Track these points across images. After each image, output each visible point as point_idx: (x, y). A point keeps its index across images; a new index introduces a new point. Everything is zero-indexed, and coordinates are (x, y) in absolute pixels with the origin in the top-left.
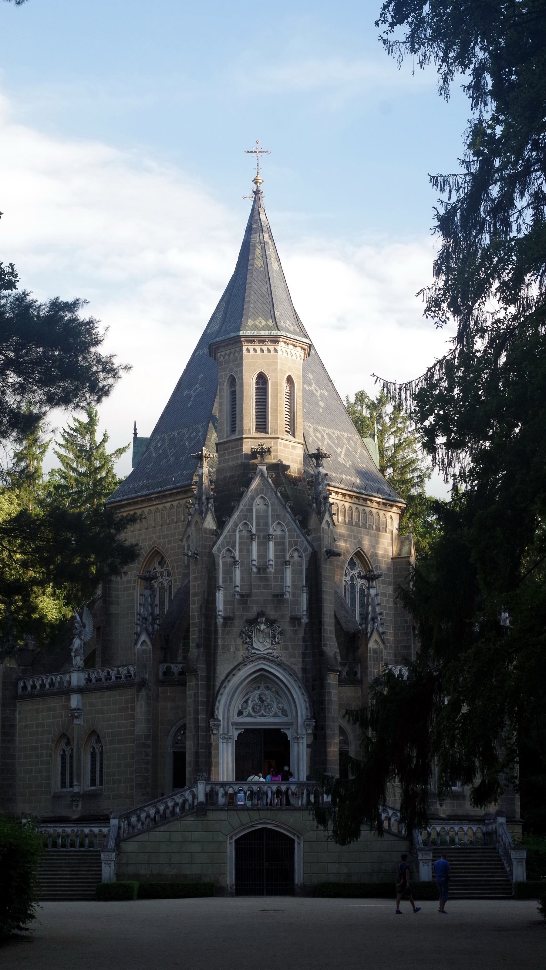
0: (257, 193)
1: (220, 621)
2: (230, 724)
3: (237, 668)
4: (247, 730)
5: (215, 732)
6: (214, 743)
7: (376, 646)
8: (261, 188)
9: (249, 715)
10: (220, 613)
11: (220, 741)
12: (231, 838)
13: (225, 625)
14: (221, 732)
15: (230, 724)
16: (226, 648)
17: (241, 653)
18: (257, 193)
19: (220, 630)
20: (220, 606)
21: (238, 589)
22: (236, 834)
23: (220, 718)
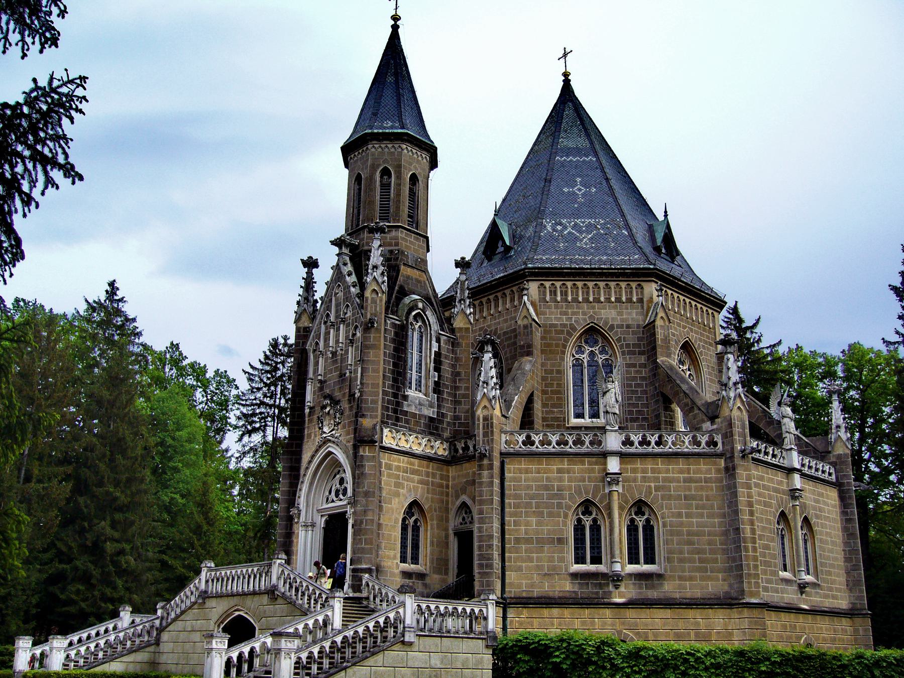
0: (395, 28)
1: (307, 411)
2: (315, 510)
3: (313, 457)
4: (330, 515)
5: (296, 520)
6: (296, 532)
7: (486, 412)
8: (398, 23)
9: (333, 501)
10: (309, 404)
11: (300, 529)
12: (219, 626)
13: (310, 414)
14: (301, 520)
15: (315, 510)
16: (309, 436)
17: (318, 440)
18: (395, 28)
19: (307, 419)
20: (309, 397)
21: (319, 378)
22: (222, 622)
23: (301, 507)
